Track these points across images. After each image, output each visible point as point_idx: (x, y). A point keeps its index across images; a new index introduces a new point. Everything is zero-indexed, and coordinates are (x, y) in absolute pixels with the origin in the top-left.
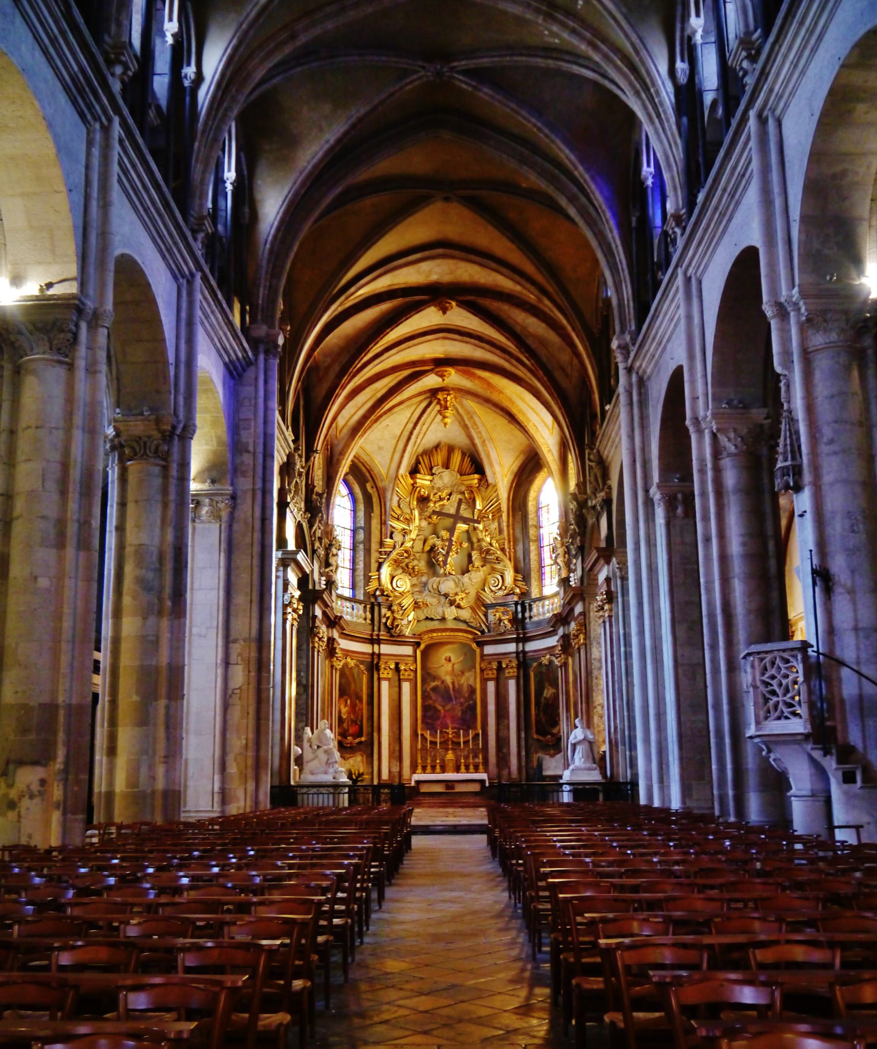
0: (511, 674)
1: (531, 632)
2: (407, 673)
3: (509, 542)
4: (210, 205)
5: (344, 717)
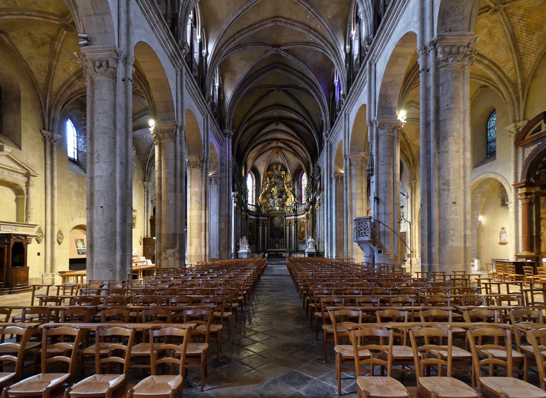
4: (212, 94)
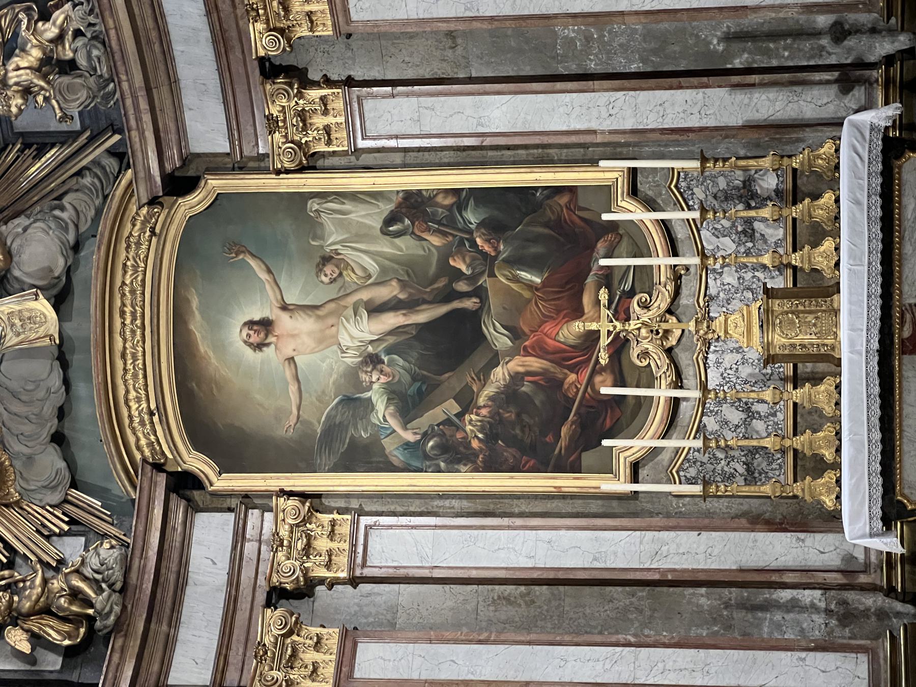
2: (322, 544)
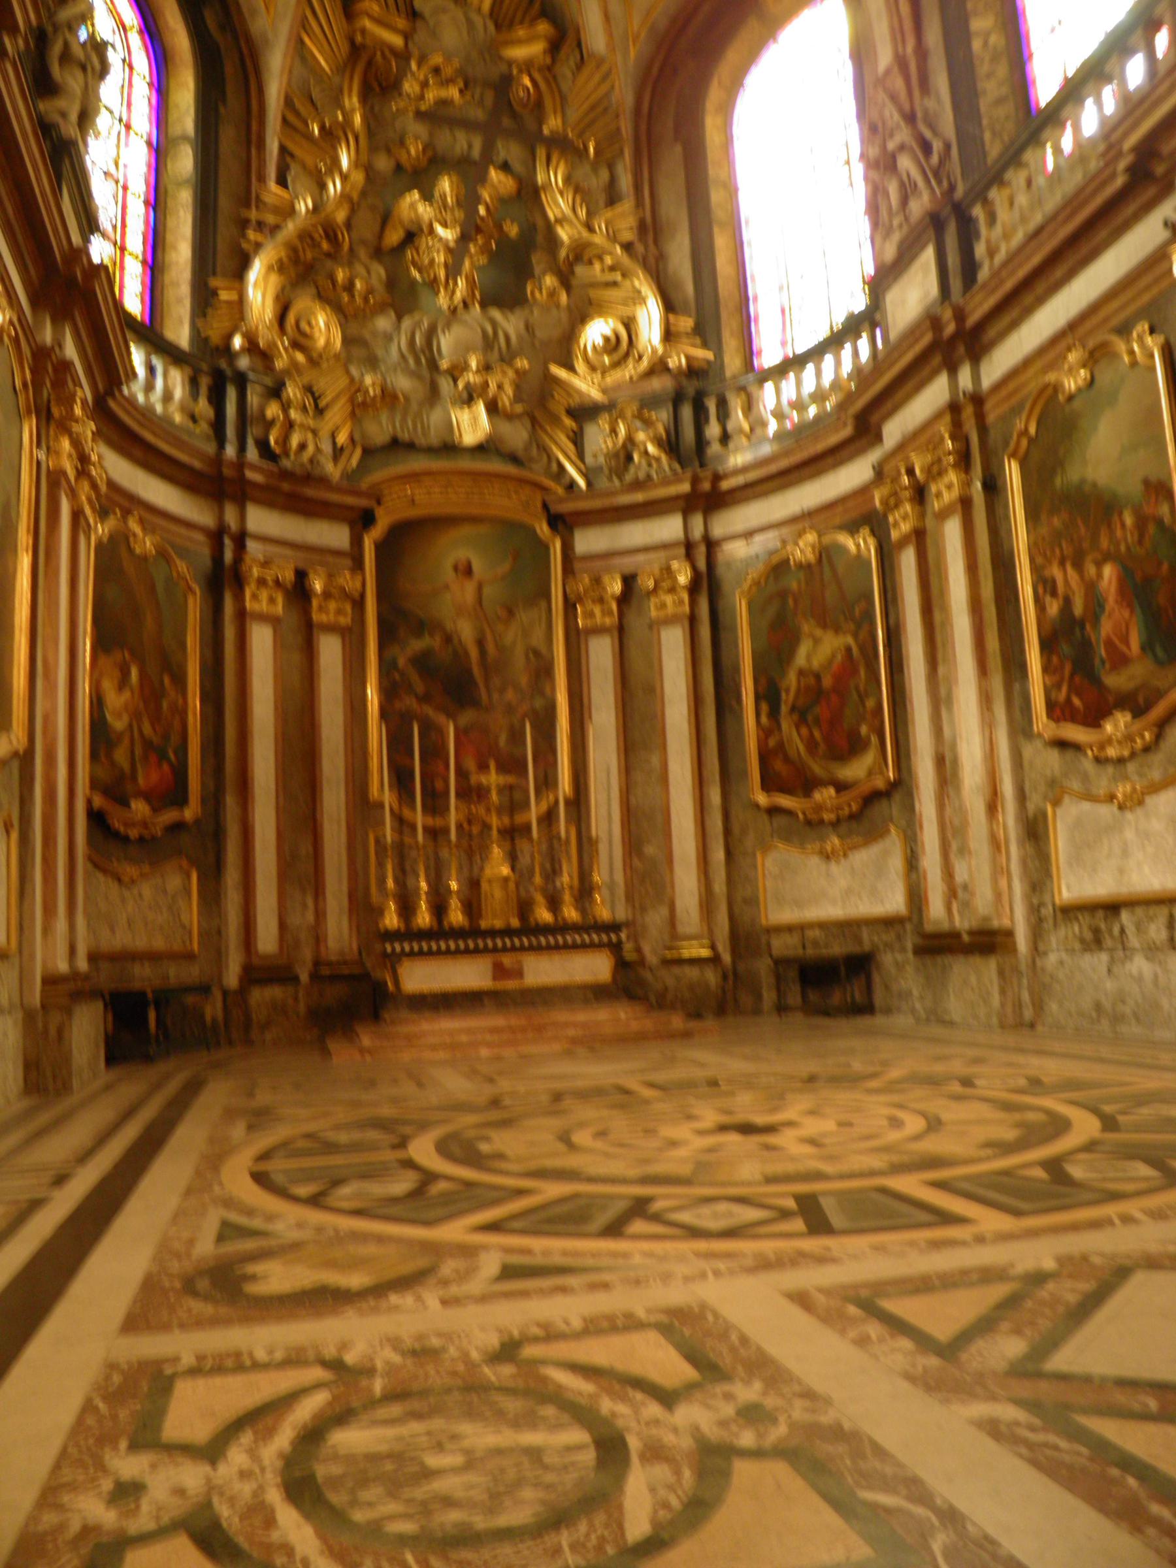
0: (670, 609)
1: (745, 469)
2: (332, 605)
3: (642, 228)
5: (118, 724)
